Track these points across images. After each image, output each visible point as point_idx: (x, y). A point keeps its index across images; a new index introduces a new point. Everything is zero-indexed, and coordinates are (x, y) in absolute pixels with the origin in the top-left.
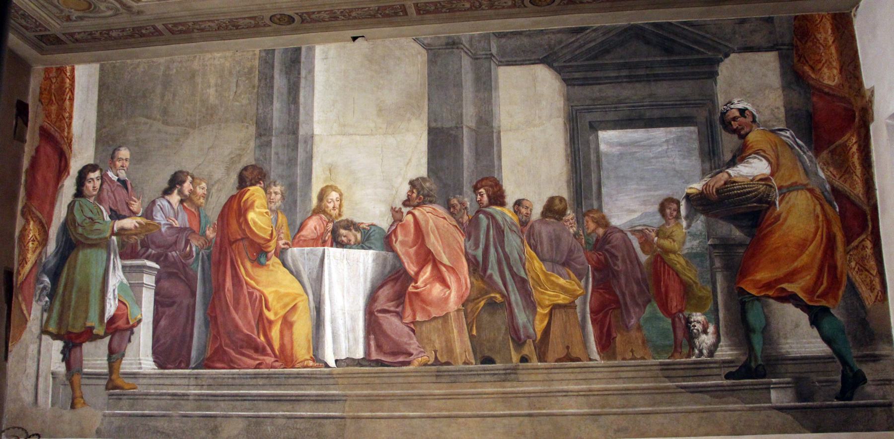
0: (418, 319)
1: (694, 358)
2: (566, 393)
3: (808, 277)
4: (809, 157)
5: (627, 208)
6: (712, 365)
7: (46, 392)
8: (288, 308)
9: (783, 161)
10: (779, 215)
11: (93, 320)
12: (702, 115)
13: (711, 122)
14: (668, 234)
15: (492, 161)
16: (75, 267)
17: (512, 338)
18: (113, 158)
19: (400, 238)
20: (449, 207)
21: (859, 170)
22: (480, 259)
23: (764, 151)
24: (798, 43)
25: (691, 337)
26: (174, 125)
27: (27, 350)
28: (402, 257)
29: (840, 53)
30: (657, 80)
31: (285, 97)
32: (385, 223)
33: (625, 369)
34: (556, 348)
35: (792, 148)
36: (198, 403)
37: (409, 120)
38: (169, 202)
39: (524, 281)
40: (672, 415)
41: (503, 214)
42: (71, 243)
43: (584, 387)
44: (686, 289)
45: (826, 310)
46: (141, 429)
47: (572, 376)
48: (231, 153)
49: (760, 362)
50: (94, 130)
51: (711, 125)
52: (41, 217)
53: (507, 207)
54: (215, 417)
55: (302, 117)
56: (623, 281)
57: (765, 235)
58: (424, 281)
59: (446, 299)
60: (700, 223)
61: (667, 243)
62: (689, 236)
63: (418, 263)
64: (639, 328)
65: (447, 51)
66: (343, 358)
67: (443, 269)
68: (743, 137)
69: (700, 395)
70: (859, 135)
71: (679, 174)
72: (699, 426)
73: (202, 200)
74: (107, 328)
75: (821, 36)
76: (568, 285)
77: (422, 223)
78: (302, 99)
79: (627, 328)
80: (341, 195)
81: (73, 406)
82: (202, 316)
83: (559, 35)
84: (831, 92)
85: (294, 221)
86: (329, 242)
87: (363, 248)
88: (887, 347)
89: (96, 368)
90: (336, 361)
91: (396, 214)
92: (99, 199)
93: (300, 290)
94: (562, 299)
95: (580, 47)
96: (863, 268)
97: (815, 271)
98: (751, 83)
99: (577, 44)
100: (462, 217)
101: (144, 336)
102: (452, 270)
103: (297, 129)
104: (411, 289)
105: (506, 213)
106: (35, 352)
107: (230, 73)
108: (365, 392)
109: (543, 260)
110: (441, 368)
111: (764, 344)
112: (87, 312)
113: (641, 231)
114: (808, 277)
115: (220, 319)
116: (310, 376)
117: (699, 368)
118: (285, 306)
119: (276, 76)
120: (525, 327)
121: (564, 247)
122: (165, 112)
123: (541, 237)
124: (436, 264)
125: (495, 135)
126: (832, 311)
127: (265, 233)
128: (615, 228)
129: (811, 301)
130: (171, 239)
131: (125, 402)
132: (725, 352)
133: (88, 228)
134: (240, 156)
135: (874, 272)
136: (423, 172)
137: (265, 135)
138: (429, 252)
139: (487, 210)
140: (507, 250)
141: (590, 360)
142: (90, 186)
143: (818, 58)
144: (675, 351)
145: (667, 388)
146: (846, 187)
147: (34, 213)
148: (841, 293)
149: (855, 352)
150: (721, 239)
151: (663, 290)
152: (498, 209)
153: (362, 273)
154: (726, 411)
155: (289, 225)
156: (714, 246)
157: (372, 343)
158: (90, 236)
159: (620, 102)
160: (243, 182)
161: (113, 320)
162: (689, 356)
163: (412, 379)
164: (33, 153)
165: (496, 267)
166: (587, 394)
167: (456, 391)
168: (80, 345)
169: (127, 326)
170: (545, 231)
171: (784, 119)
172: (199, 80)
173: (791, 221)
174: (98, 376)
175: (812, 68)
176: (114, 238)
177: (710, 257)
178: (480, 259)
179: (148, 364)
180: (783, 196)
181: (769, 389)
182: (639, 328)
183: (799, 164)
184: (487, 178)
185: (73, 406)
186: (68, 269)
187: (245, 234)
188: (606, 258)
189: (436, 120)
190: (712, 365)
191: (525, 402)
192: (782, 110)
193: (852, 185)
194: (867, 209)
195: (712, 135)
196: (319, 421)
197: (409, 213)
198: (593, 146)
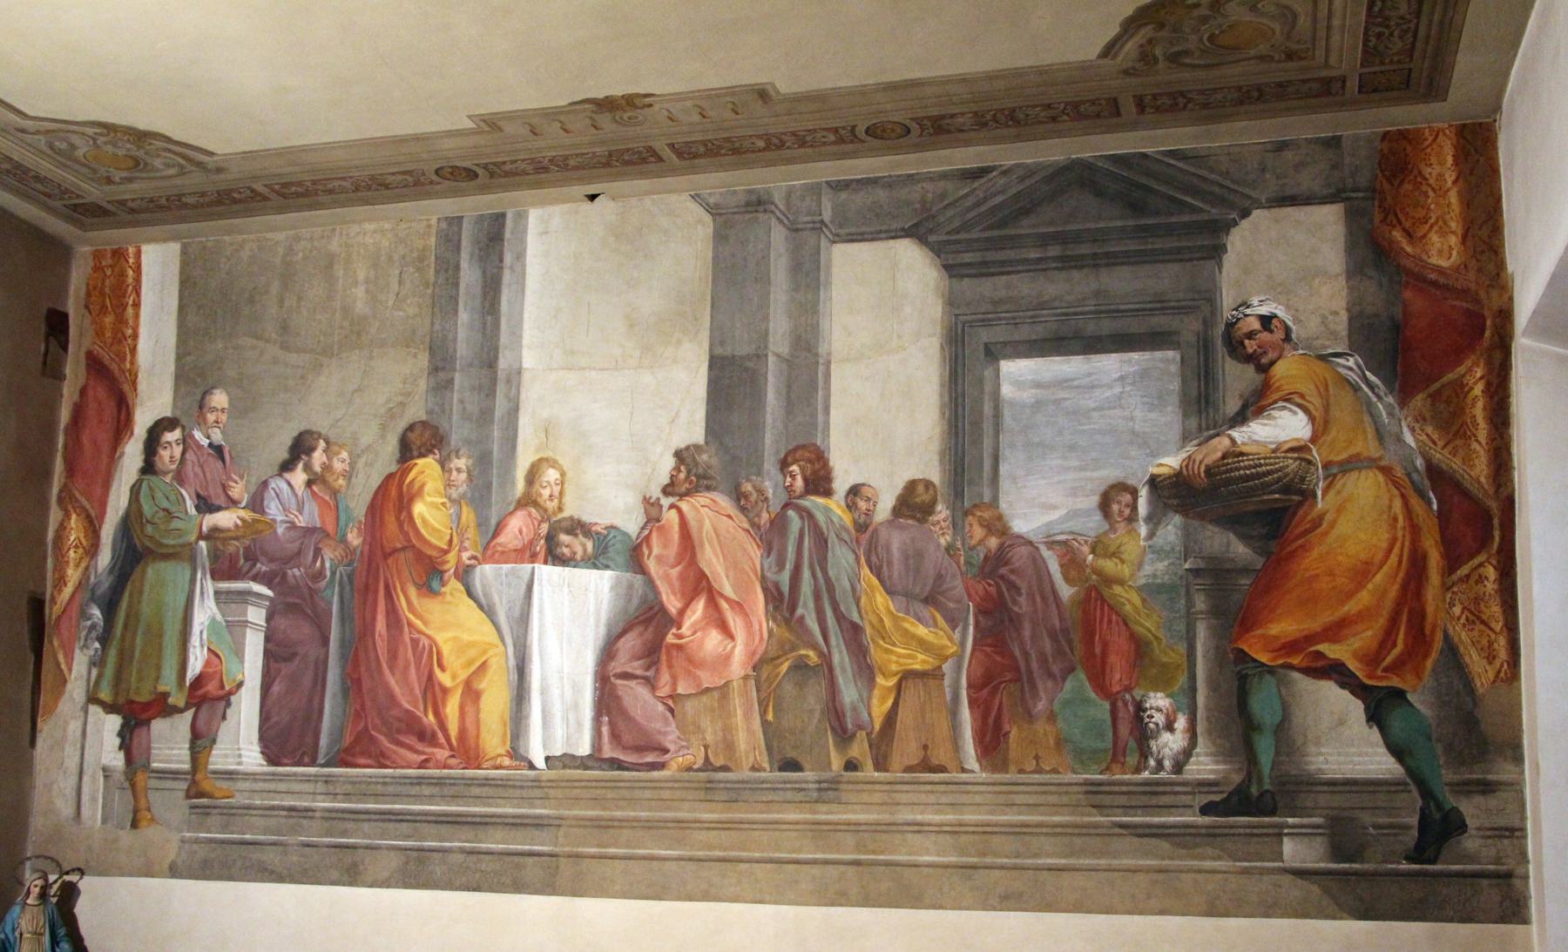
0: (680, 690)
1: (1146, 774)
2: (919, 828)
3: (1369, 633)
4: (1388, 407)
5: (1042, 502)
6: (1177, 789)
7: (94, 800)
8: (473, 668)
9: (1335, 412)
10: (1321, 517)
11: (168, 683)
12: (1189, 327)
13: (1206, 340)
14: (1112, 549)
15: (814, 416)
16: (141, 592)
17: (833, 729)
18: (201, 407)
19: (656, 551)
20: (738, 496)
21: (1483, 431)
22: (786, 589)
23: (1302, 396)
24: (1386, 186)
25: (1143, 735)
26: (299, 351)
27: (65, 730)
28: (658, 583)
29: (1467, 203)
30: (1114, 264)
31: (478, 301)
32: (631, 524)
33: (1022, 788)
34: (906, 749)
35: (1356, 389)
36: (326, 824)
37: (679, 342)
38: (289, 484)
39: (856, 629)
40: (1103, 875)
41: (827, 510)
42: (135, 553)
43: (950, 817)
44: (1140, 649)
45: (1399, 694)
46: (239, 863)
47: (932, 799)
48: (389, 400)
49: (1267, 787)
50: (172, 357)
51: (1206, 347)
53: (836, 497)
54: (354, 847)
55: (504, 339)
56: (1027, 633)
57: (1292, 554)
58: (693, 625)
59: (727, 658)
60: (1172, 530)
61: (1109, 566)
62: (1150, 552)
63: (683, 594)
64: (1052, 717)
65: (747, 216)
66: (558, 754)
67: (724, 605)
68: (1264, 369)
69: (1154, 841)
70: (1489, 363)
71: (1140, 440)
72: (1149, 897)
73: (341, 481)
74: (191, 695)
75: (1431, 172)
76: (931, 638)
77: (693, 523)
78: (504, 306)
79: (1030, 717)
80: (563, 474)
81: (135, 824)
82: (338, 678)
83: (942, 184)
84: (1442, 280)
85: (487, 519)
86: (542, 556)
87: (595, 567)
88: (1511, 767)
89: (170, 762)
90: (547, 759)
91: (652, 511)
92: (180, 477)
93: (492, 637)
94: (920, 662)
95: (978, 204)
96: (1475, 617)
97: (1382, 621)
98: (1289, 267)
99: (968, 203)
100: (759, 516)
101: (246, 709)
102: (738, 606)
103: (496, 358)
104: (670, 639)
105: (832, 509)
106: (79, 733)
107: (390, 258)
108: (591, 813)
109: (890, 592)
110: (712, 777)
111: (1277, 753)
112: (159, 668)
113: (1065, 543)
114: (1369, 633)
115: (366, 684)
116: (503, 784)
117: (1156, 793)
118: (470, 663)
119: (464, 264)
120: (854, 709)
121: (929, 569)
122: (285, 328)
123: (888, 551)
124: (713, 596)
125: (821, 368)
126: (1409, 697)
127: (441, 539)
128: (1019, 537)
129: (1370, 677)
131: (215, 820)
132: (1204, 766)
133: (162, 527)
134: (402, 404)
135: (1498, 626)
136: (697, 435)
137: (443, 369)
138: (702, 576)
139: (803, 502)
140: (831, 573)
141: (964, 770)
142: (165, 454)
143: (1420, 213)
144: (1114, 759)
145: (1096, 826)
146: (1456, 465)
147: (77, 500)
148: (1429, 663)
149: (1448, 776)
150: (1210, 558)
151: (1098, 650)
152: (820, 500)
153: (592, 608)
154: (1200, 871)
155: (479, 525)
156: (1196, 572)
157: (605, 730)
158: (165, 541)
159: (1042, 306)
160: (408, 451)
161: (199, 681)
162: (1138, 770)
163: (666, 794)
164: (76, 397)
165: (811, 605)
166: (956, 830)
167: (738, 816)
168: (147, 722)
169: (221, 693)
170: (896, 541)
171: (1345, 333)
172: (339, 271)
173: (1344, 527)
174: (174, 774)
175: (1409, 235)
176: (203, 544)
177: (1188, 592)
178: (786, 589)
179: (251, 757)
180: (1331, 480)
181: (1280, 835)
182: (1052, 717)
183: (1367, 418)
184: (803, 447)
185: (135, 824)
186: (131, 596)
187: (409, 541)
188: (1000, 593)
189: (722, 343)
190: (1177, 789)
191: (849, 839)
192: (1344, 316)
193: (1468, 460)
194: (1493, 505)
195: (1206, 365)
196: (516, 859)
197: (672, 506)
198: (988, 388)
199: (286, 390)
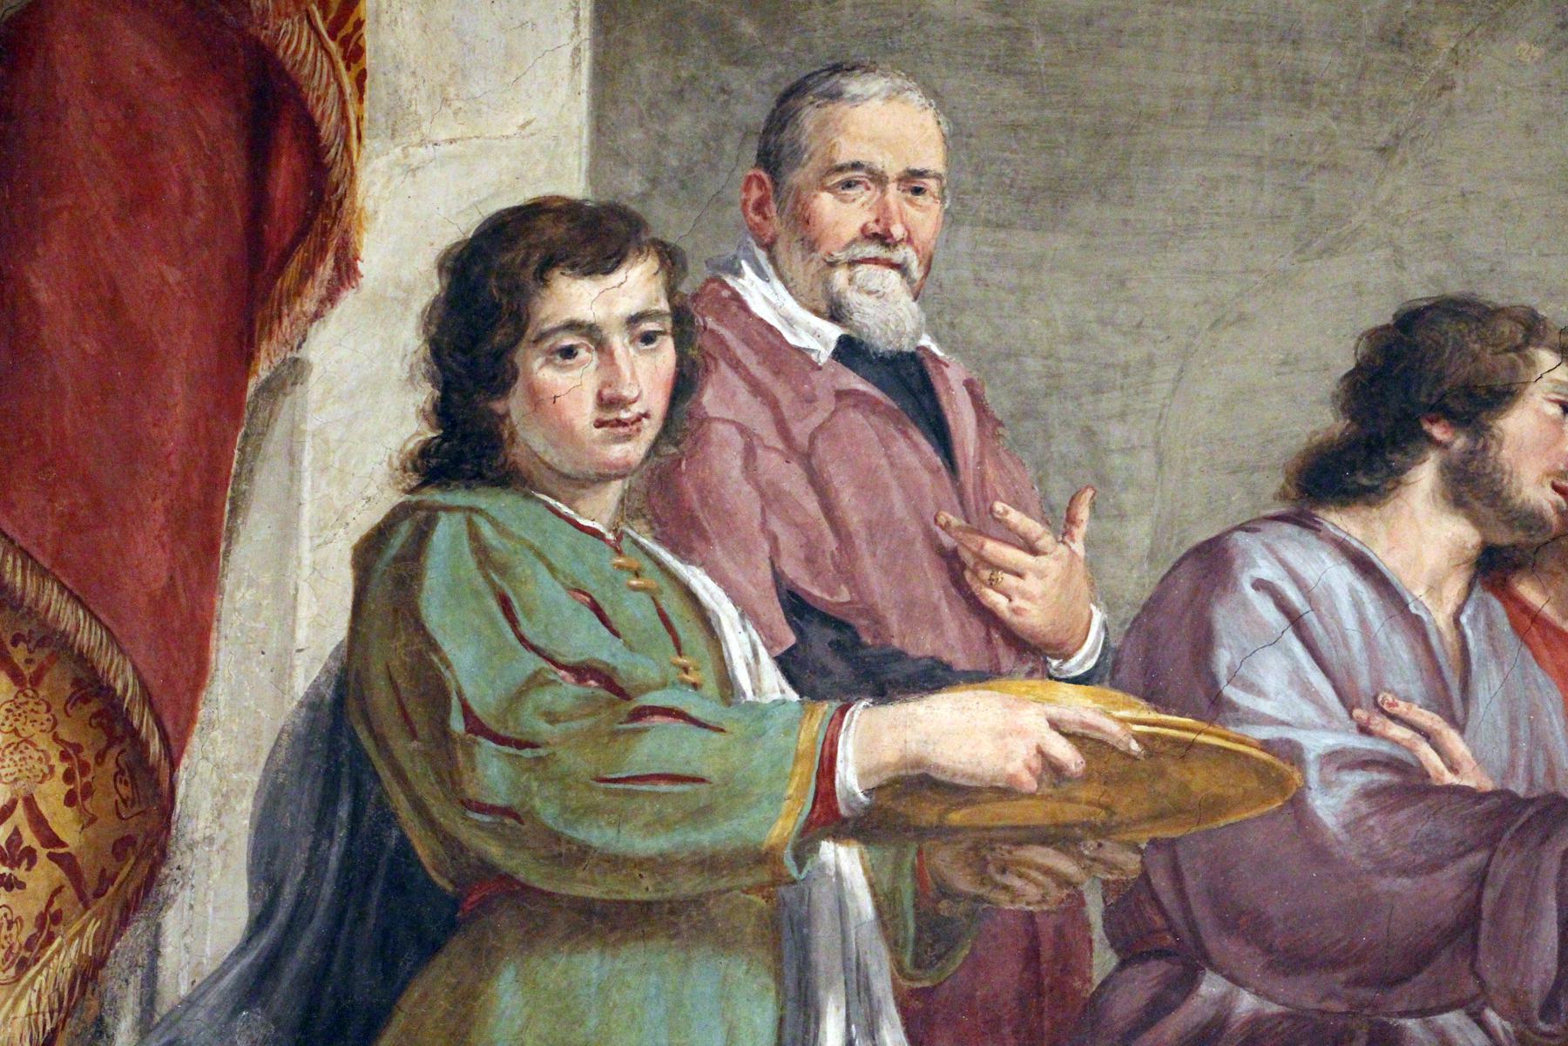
18: (774, 153)
38: (1364, 566)
52: (89, 637)
92: (670, 500)
130: (1420, 897)
142: (571, 387)
158: (597, 835)
176: (843, 859)
199: (1301, 91)
